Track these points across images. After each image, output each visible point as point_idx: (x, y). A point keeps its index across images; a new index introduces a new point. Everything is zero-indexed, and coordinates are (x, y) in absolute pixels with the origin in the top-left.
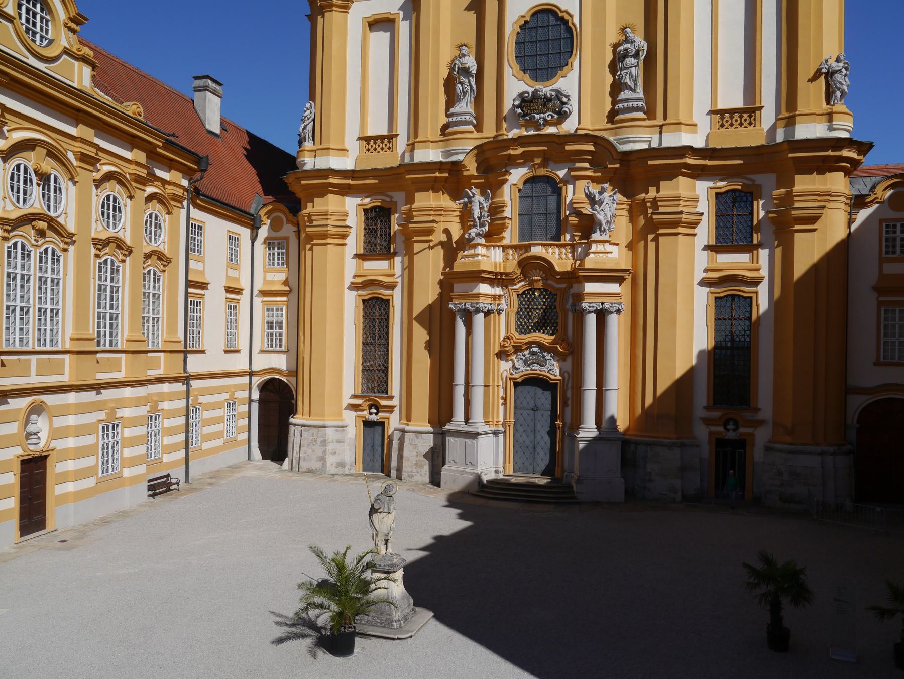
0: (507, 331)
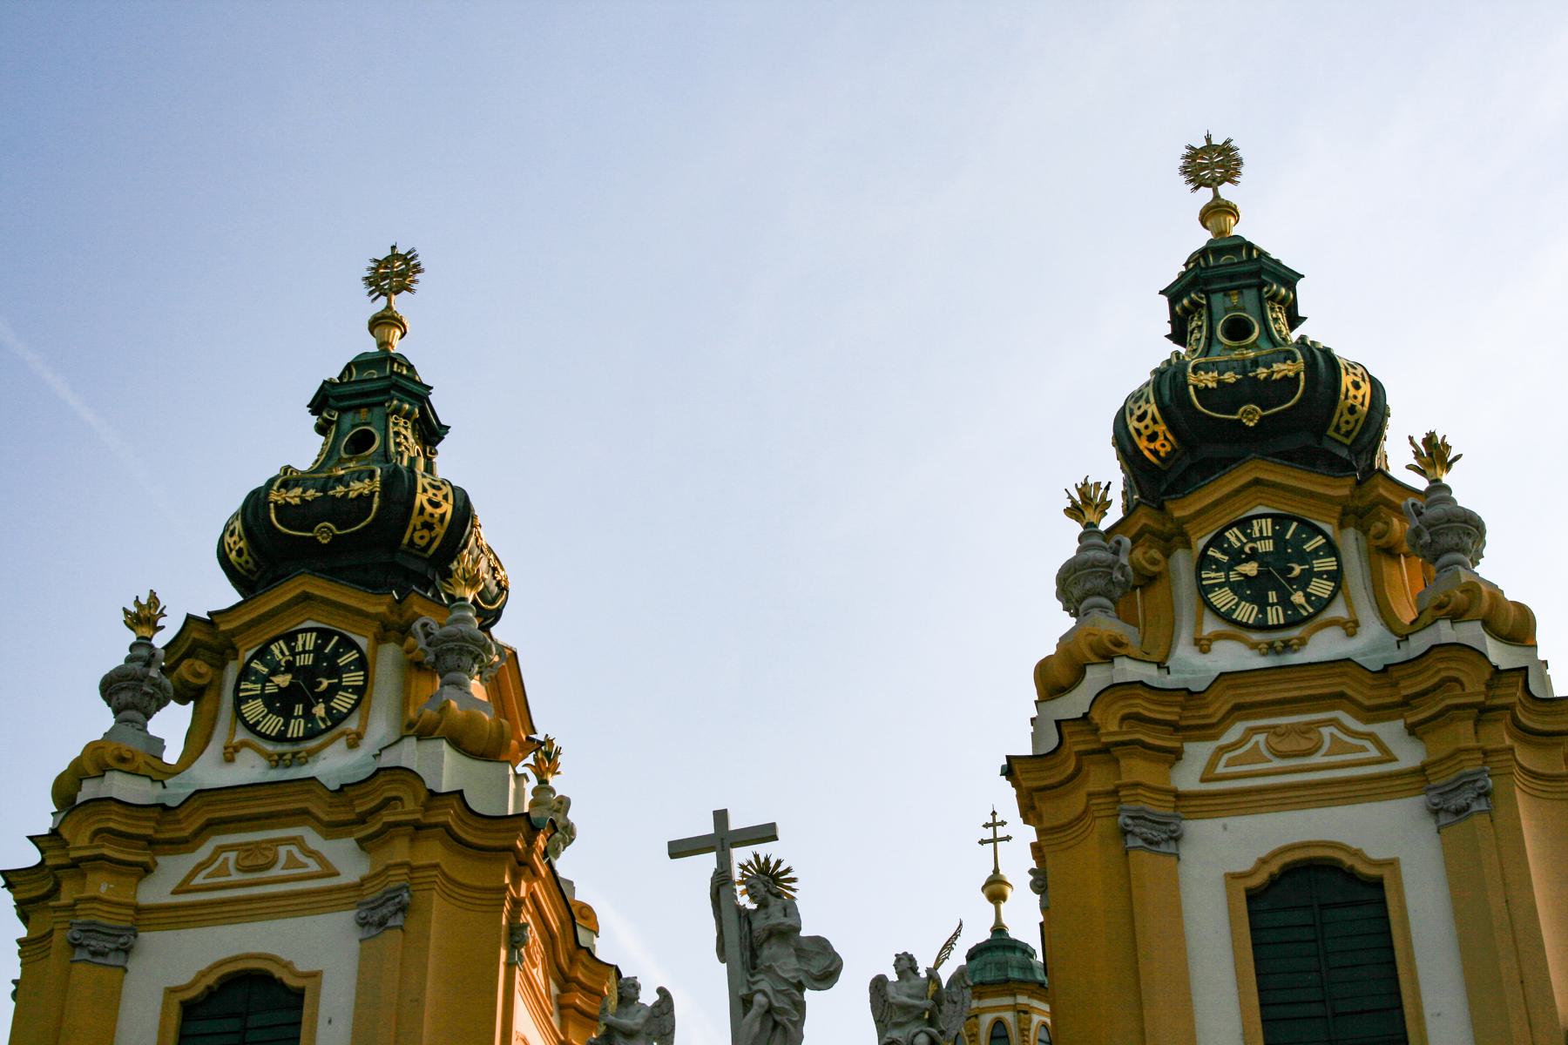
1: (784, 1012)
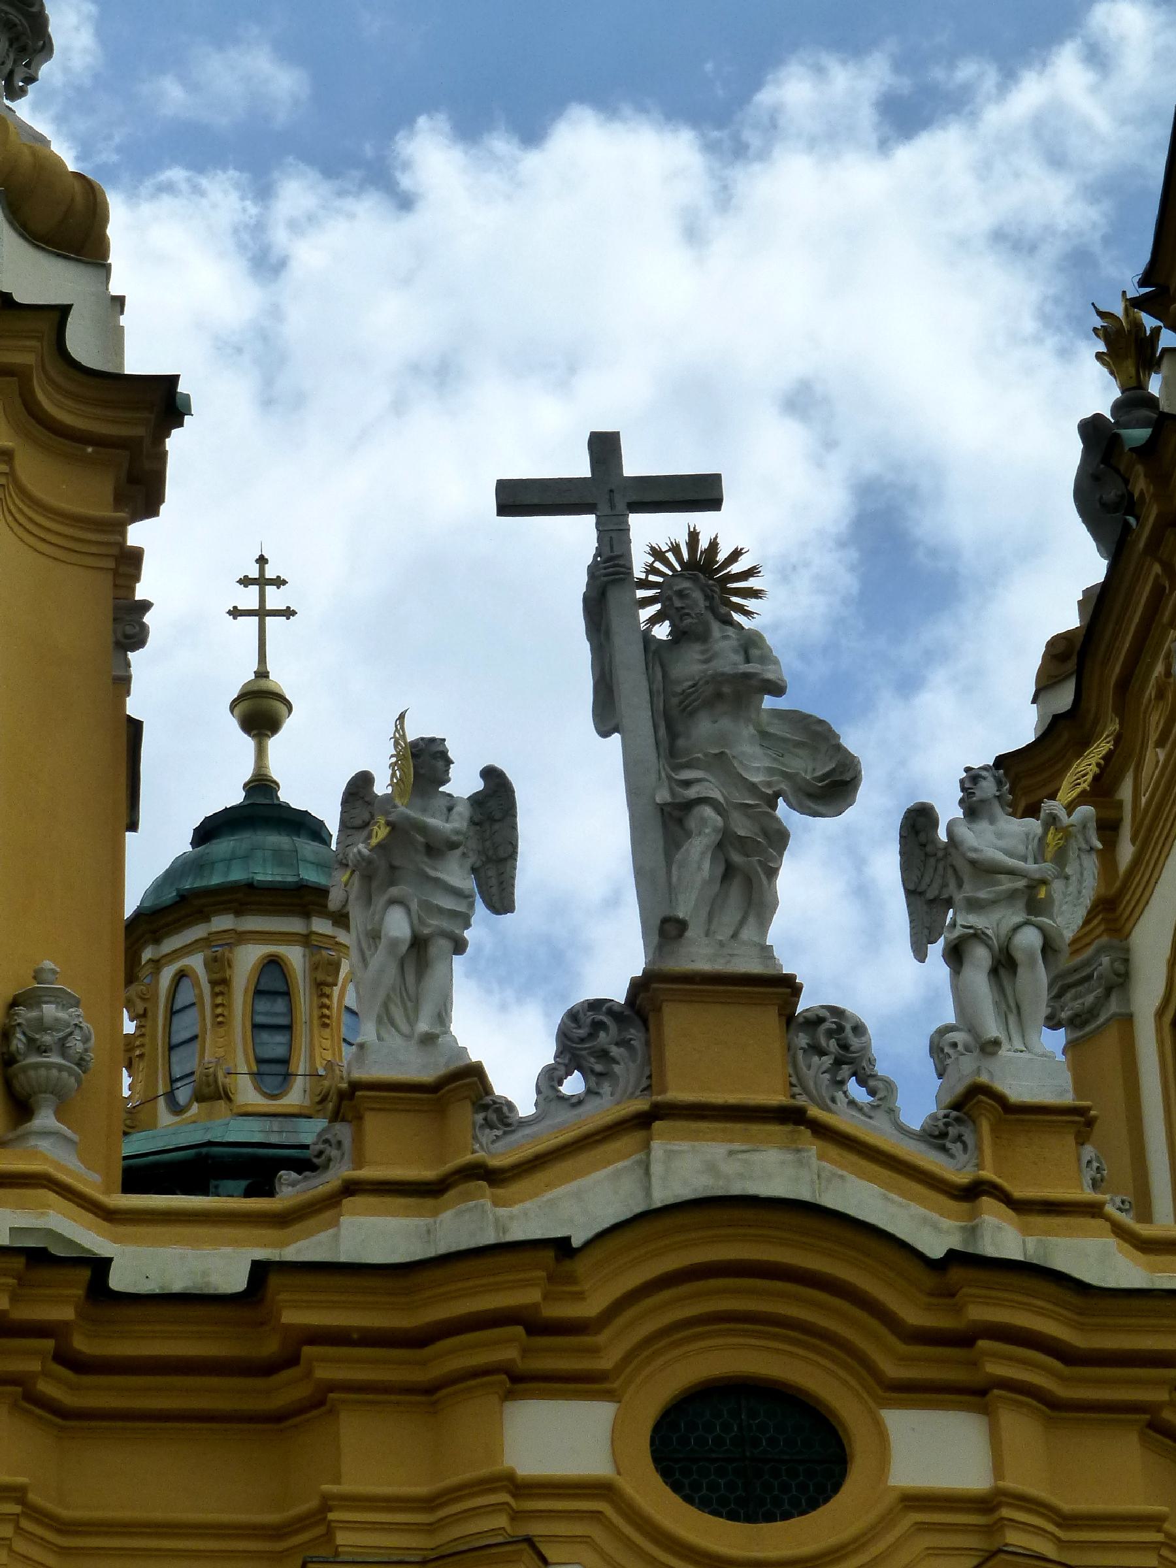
1: (743, 844)
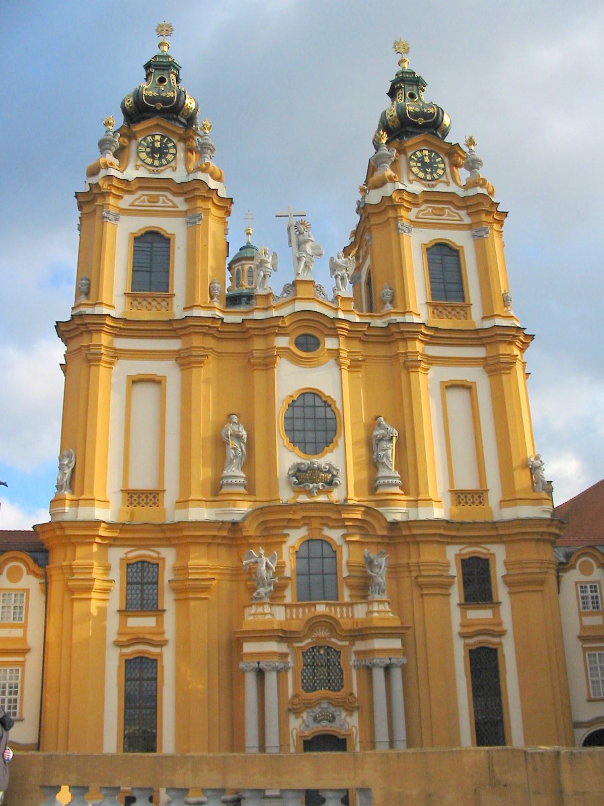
0: (294, 689)
1: (308, 262)
